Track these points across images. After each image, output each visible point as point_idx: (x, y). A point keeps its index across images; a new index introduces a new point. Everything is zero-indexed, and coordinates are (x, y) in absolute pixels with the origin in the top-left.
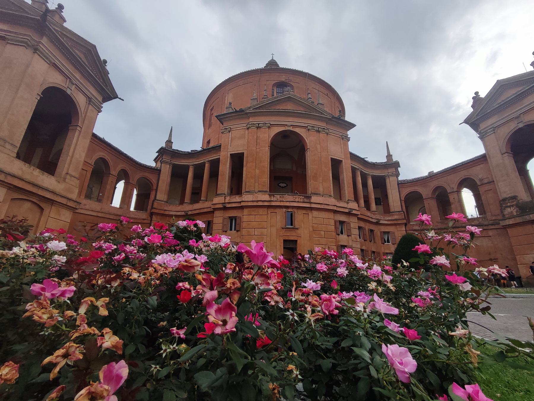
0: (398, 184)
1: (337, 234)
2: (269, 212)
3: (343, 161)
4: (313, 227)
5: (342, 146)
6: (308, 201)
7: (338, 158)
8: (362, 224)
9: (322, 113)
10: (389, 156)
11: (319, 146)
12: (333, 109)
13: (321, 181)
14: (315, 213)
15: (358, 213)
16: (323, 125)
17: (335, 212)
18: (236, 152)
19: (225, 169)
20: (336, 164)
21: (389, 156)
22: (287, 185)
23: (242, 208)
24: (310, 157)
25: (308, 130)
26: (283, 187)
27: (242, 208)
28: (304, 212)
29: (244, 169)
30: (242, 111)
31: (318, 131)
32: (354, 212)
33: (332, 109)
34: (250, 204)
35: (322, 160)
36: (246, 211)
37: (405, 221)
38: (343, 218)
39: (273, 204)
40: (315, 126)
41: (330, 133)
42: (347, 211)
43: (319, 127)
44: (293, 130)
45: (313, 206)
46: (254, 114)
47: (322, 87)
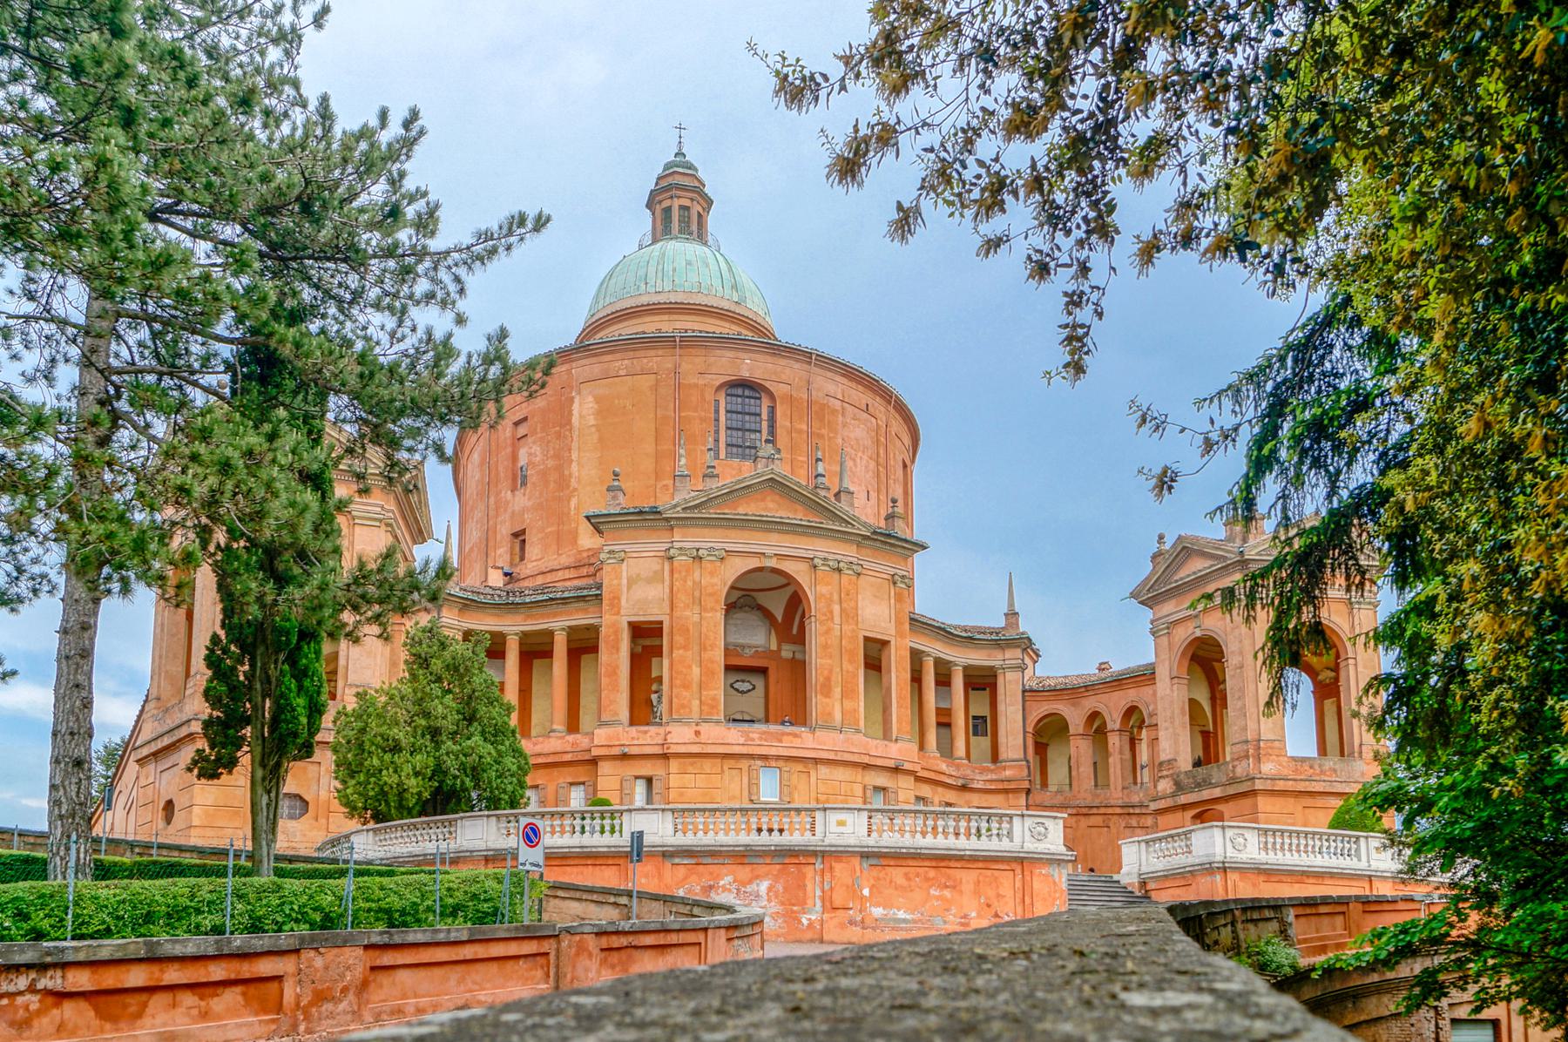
11: (836, 608)
14: (824, 771)
17: (866, 767)
19: (616, 657)
23: (665, 757)
26: (743, 692)
27: (665, 757)
28: (800, 767)
29: (666, 662)
30: (655, 511)
32: (907, 766)
34: (682, 749)
36: (674, 765)
40: (831, 557)
42: (891, 764)
47: (854, 385)
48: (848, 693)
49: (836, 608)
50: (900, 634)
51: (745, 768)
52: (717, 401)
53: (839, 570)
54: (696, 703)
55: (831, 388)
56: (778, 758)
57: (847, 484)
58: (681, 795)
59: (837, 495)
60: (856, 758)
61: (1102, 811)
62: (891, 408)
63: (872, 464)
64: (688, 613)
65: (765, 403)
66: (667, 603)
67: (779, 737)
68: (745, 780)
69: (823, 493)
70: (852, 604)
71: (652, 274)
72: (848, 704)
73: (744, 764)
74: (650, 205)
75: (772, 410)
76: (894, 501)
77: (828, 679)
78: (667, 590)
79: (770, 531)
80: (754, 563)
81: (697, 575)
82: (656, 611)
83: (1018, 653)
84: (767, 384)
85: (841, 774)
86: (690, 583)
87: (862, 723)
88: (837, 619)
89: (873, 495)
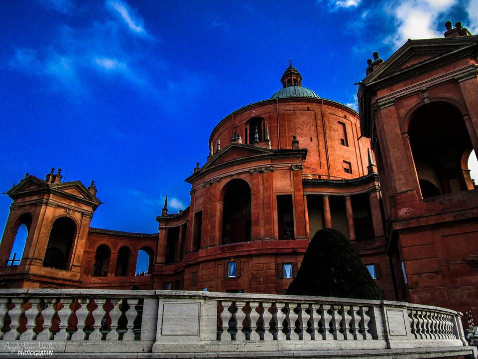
1: (279, 278)
4: (252, 274)
5: (292, 178)
9: (262, 152)
11: (261, 188)
14: (255, 260)
16: (268, 163)
20: (285, 202)
23: (198, 264)
25: (251, 173)
31: (261, 172)
33: (316, 123)
35: (265, 201)
36: (201, 266)
41: (276, 169)
42: (290, 251)
43: (261, 167)
46: (208, 172)
49: (261, 188)
50: (296, 190)
55: (288, 108)
56: (234, 257)
60: (269, 252)
67: (234, 248)
68: (223, 268)
70: (269, 184)
72: (267, 227)
77: (258, 218)
79: (234, 165)
80: (229, 180)
81: (211, 191)
84: (261, 116)
85: (263, 260)
86: (209, 194)
88: (261, 192)
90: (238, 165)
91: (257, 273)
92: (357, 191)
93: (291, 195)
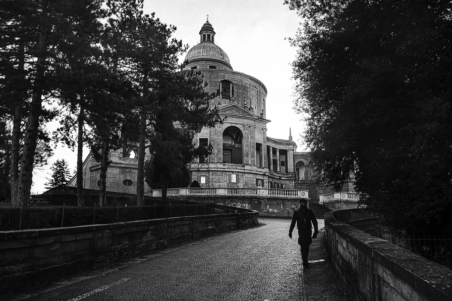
0: (294, 156)
2: (223, 174)
3: (263, 144)
4: (245, 182)
5: (263, 134)
6: (243, 168)
7: (260, 143)
8: (271, 180)
10: (291, 137)
11: (249, 136)
12: (259, 97)
13: (250, 157)
14: (246, 175)
15: (269, 174)
18: (203, 138)
20: (259, 146)
21: (291, 137)
22: (228, 154)
24: (244, 141)
25: (244, 126)
26: (226, 155)
32: (266, 174)
34: (213, 169)
37: (294, 178)
38: (260, 177)
39: (226, 170)
40: (248, 124)
42: (263, 173)
43: (250, 124)
44: (235, 126)
45: (246, 171)
47: (252, 81)
48: (252, 156)
49: (249, 136)
50: (264, 142)
51: (228, 174)
52: (220, 85)
53: (250, 127)
54: (216, 158)
56: (236, 172)
57: (252, 106)
58: (212, 180)
59: (249, 109)
61: (313, 185)
62: (261, 86)
63: (257, 100)
64: (214, 137)
65: (231, 85)
66: (209, 134)
68: (228, 177)
69: (246, 109)
71: (201, 51)
73: (228, 173)
74: (200, 33)
75: (233, 87)
76: (262, 110)
78: (209, 131)
79: (234, 117)
80: (230, 125)
82: (206, 136)
83: (292, 146)
84: (232, 81)
85: (251, 176)
87: (256, 163)
88: (250, 139)
89: (257, 107)
90: (236, 118)
91: (248, 182)
92: (283, 147)
93: (262, 144)
